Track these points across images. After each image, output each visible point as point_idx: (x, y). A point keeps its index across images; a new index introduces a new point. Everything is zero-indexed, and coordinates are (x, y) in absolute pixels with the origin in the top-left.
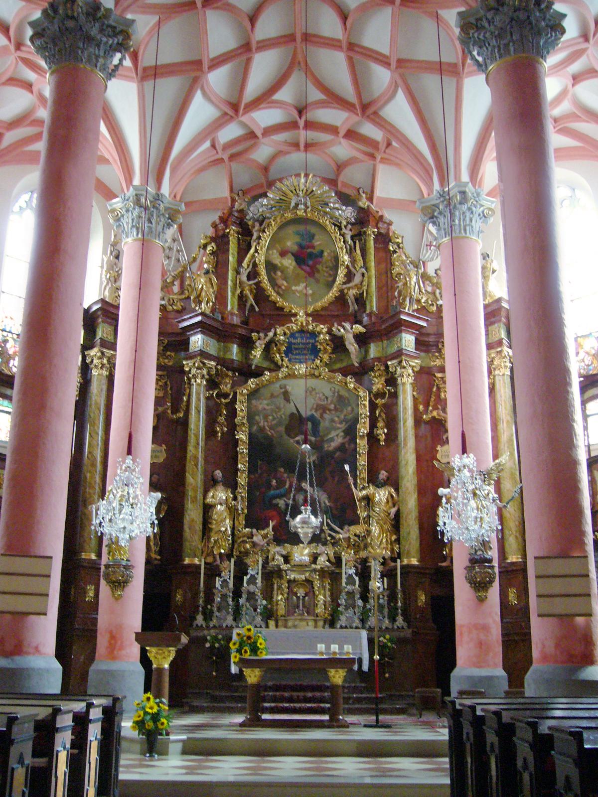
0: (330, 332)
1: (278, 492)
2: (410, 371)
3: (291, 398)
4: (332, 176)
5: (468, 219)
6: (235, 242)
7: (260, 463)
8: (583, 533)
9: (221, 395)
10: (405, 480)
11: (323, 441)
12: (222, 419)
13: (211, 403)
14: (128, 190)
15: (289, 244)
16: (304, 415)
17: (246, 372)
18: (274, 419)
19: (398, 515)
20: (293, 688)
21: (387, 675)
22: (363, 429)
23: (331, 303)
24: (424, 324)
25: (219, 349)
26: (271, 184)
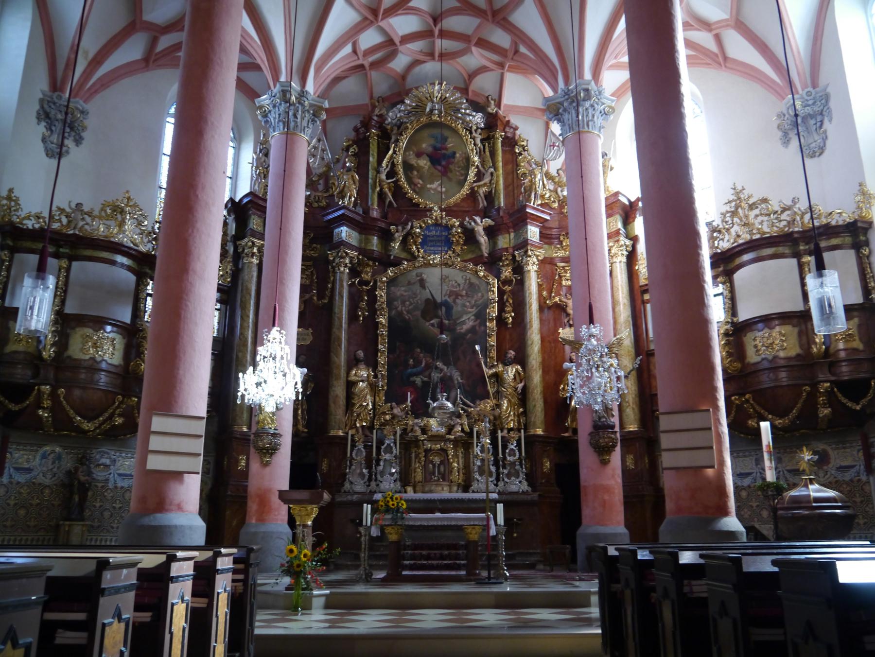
0: (461, 225)
1: (415, 370)
2: (535, 260)
3: (427, 285)
4: (462, 86)
5: (590, 115)
6: (376, 144)
7: (398, 344)
8: (715, 389)
10: (531, 358)
11: (455, 324)
14: (275, 87)
15: (424, 146)
16: (439, 300)
17: (386, 261)
18: (411, 304)
19: (525, 388)
20: (430, 547)
23: (463, 200)
24: (548, 217)
25: (360, 241)
26: (407, 92)
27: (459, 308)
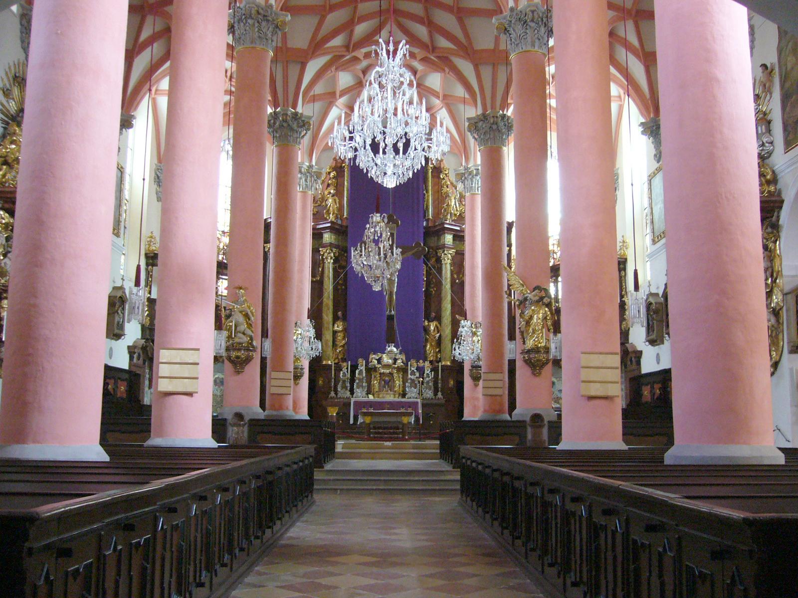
2: (450, 256)
20: (384, 428)
21: (431, 422)
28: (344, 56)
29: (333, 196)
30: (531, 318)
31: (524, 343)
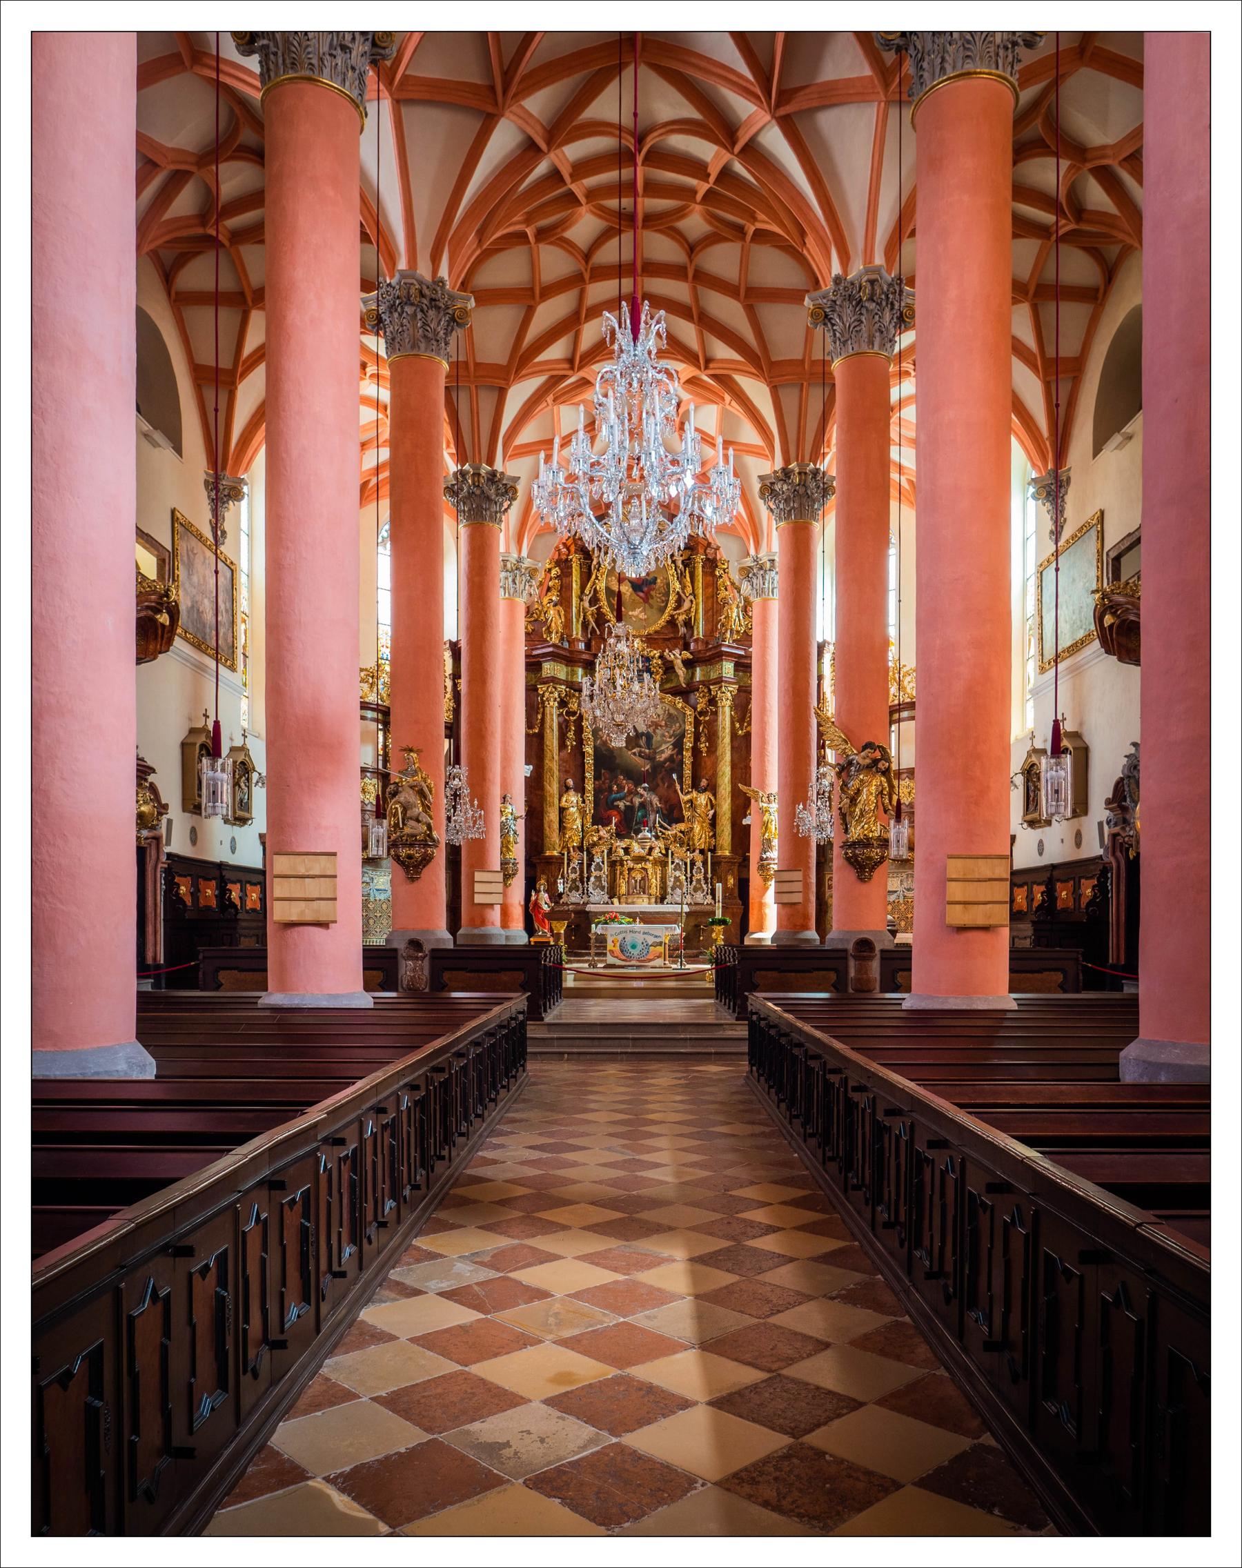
9: (570, 713)
11: (655, 753)
12: (571, 735)
13: (561, 719)
19: (715, 815)
22: (688, 744)
27: (659, 738)
28: (565, 377)
29: (555, 605)
30: (858, 792)
31: (846, 831)
